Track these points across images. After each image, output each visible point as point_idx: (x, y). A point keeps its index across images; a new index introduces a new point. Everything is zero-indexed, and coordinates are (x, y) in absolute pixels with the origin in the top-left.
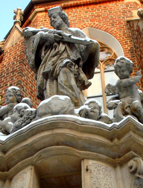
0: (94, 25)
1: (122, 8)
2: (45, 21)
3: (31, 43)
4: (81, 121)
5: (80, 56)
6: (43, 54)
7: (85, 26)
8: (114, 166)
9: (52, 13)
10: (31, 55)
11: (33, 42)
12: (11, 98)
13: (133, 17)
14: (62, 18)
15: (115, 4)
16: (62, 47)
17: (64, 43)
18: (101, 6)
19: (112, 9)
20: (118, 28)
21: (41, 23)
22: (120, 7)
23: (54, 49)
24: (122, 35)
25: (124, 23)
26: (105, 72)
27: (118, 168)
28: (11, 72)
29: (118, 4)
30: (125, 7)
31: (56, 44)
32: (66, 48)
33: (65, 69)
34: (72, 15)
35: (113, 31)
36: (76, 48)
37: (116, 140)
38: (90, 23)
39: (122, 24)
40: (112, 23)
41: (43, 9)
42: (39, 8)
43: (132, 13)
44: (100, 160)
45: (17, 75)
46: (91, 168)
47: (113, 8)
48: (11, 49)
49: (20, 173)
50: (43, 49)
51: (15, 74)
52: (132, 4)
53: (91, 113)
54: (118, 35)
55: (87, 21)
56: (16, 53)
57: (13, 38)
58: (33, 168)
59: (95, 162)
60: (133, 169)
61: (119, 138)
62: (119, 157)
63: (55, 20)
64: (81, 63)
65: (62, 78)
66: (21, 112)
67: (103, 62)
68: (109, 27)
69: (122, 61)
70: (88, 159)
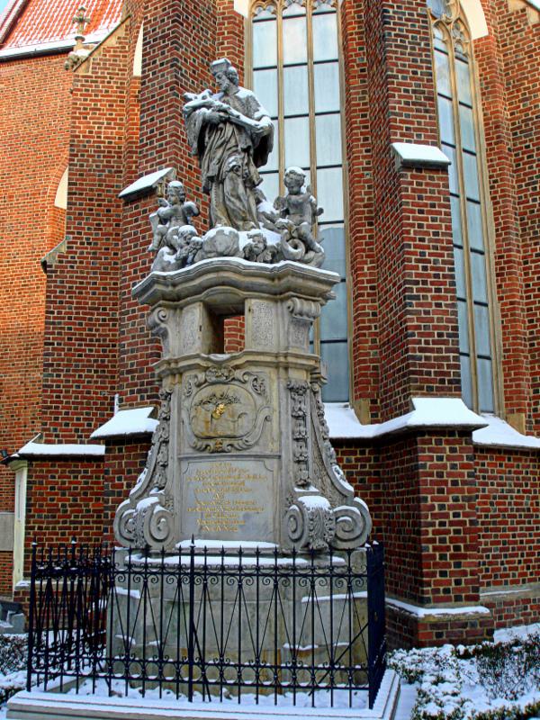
4: (244, 266)
5: (250, 144)
6: (207, 139)
8: (276, 301)
12: (173, 199)
16: (229, 129)
17: (231, 123)
23: (219, 132)
26: (314, 14)
31: (221, 125)
32: (233, 131)
33: (231, 174)
36: (245, 131)
37: (276, 281)
44: (262, 298)
46: (254, 308)
50: (207, 131)
53: (256, 249)
58: (201, 304)
62: (281, 294)
63: (220, 81)
64: (252, 152)
65: (228, 186)
69: (291, 175)
70: (251, 298)
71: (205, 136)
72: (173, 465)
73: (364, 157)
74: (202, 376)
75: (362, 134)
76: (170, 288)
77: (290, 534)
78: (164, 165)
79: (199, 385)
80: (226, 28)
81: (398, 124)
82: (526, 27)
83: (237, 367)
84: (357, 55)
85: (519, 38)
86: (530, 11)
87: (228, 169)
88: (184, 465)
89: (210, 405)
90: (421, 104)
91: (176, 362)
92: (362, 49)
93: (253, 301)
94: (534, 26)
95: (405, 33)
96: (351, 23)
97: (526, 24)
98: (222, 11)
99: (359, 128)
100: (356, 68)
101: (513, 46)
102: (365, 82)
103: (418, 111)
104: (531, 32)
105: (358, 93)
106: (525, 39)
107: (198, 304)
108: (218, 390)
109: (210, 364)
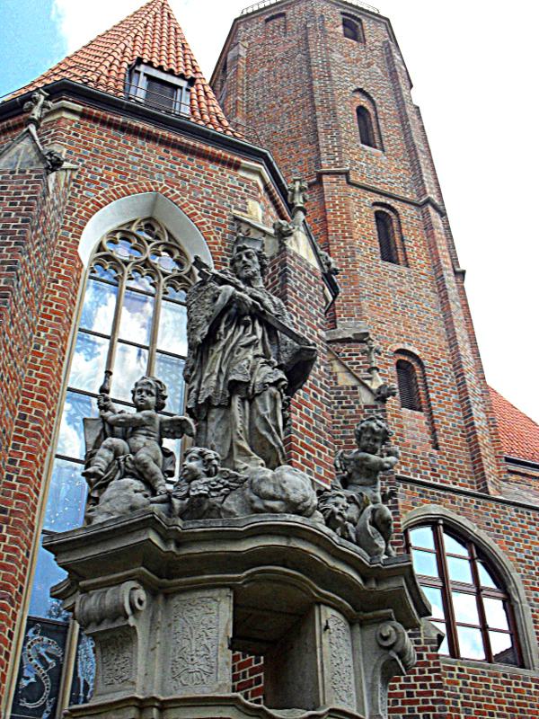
0: (172, 195)
1: (230, 183)
2: (74, 134)
3: (206, 297)
7: (152, 187)
9: (248, 246)
10: (200, 322)
11: (215, 299)
13: (246, 212)
14: (260, 263)
15: (220, 170)
18: (192, 160)
19: (212, 175)
20: (216, 224)
21: (65, 135)
22: (228, 181)
23: (242, 328)
24: (220, 241)
25: (227, 217)
27: (358, 629)
29: (225, 173)
30: (237, 185)
31: (249, 318)
33: (273, 390)
34: (134, 151)
35: (203, 223)
38: (165, 185)
39: (224, 217)
40: (206, 207)
41: (79, 108)
42: (72, 102)
43: (247, 203)
45: (12, 246)
47: (214, 175)
48: (7, 178)
50: (225, 319)
51: (8, 240)
52: (251, 185)
53: (338, 518)
54: (212, 237)
55: (159, 179)
56: (20, 193)
57: (18, 154)
59: (334, 613)
60: (390, 643)
61: (378, 581)
66: (210, 466)
67: (166, 278)
68: (199, 212)
70: (327, 605)
71: (219, 325)
76: (172, 547)
80: (64, 267)
81: (299, 447)
82: (357, 405)
85: (348, 414)
87: (271, 381)
90: (320, 433)
93: (331, 612)
94: (366, 407)
97: (357, 402)
98: (62, 246)
101: (341, 420)
103: (318, 439)
106: (355, 417)
107: (225, 591)
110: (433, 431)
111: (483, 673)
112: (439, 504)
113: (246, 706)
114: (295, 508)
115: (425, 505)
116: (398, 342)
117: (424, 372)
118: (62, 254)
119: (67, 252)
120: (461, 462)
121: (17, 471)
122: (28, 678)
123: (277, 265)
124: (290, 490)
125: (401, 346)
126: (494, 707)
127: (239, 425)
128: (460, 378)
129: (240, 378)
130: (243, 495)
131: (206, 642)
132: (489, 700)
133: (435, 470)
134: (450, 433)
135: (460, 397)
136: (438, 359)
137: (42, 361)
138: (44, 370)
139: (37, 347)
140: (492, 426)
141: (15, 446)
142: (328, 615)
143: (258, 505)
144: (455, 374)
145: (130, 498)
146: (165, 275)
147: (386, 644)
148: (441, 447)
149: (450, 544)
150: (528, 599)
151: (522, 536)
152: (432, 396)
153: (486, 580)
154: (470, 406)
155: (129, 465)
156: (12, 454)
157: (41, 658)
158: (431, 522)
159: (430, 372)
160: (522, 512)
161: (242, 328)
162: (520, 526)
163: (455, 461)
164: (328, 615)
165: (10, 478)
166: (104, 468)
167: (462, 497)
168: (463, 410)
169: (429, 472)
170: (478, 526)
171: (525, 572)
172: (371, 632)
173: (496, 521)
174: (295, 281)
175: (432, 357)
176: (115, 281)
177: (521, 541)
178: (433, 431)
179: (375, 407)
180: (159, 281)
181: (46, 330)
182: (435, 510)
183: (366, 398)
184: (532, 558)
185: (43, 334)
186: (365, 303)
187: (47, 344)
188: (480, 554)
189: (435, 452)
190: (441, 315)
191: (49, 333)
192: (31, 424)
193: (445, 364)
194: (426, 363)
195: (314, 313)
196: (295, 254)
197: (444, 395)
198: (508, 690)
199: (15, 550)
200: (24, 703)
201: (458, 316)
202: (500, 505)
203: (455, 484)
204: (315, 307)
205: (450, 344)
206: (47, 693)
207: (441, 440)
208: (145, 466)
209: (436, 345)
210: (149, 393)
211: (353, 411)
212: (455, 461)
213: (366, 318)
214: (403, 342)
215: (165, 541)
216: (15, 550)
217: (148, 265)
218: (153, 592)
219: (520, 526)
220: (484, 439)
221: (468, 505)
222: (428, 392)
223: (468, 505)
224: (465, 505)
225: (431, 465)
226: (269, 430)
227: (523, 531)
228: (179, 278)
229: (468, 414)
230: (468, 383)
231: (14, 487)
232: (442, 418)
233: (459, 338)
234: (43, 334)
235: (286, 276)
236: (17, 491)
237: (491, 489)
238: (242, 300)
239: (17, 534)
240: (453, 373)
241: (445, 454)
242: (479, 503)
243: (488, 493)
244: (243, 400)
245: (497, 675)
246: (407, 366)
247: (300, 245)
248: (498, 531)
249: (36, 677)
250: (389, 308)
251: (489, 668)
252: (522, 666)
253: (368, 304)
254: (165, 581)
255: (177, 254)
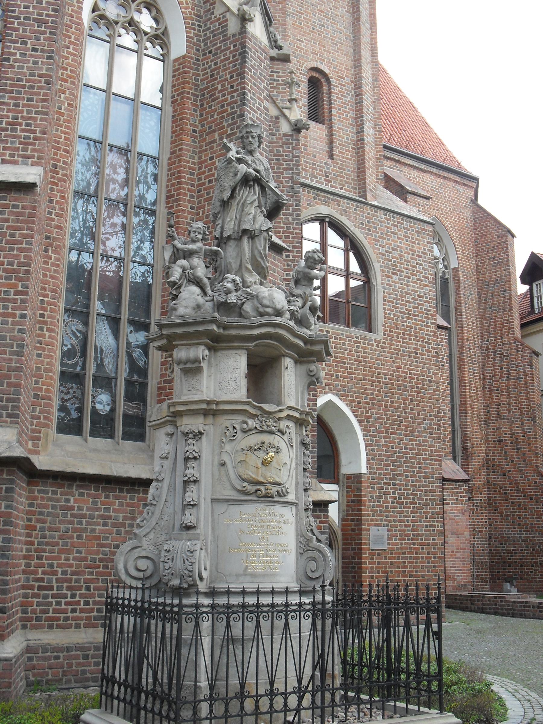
6: (237, 191)
11: (236, 175)
23: (248, 189)
24: (190, 5)
28: (35, 20)
49: (231, 351)
51: (43, 29)
53: (296, 313)
60: (313, 373)
72: (204, 506)
73: (189, 213)
74: (252, 423)
75: (189, 190)
77: (310, 575)
78: (30, 161)
79: (244, 431)
83: (280, 419)
84: (192, 115)
86: (282, 121)
88: (221, 508)
89: (261, 452)
91: (218, 403)
92: (195, 111)
94: (285, 135)
95: (255, 119)
96: (188, 83)
97: (278, 131)
99: (186, 183)
100: (189, 127)
102: (195, 142)
104: (282, 139)
105: (188, 151)
106: (275, 143)
107: (245, 351)
108: (267, 438)
109: (258, 412)
110: (331, 143)
111: (343, 335)
112: (329, 206)
113: (254, 406)
114: (279, 313)
115: (317, 206)
116: (312, 60)
117: (330, 89)
118: (71, 21)
119: (74, 19)
120: (349, 171)
121: (54, 208)
122: (66, 346)
123: (238, 43)
124: (277, 303)
125: (314, 64)
126: (346, 359)
127: (247, 255)
128: (358, 98)
129: (248, 227)
130: (253, 302)
131: (235, 374)
132: (344, 353)
133: (328, 177)
134: (344, 146)
135: (356, 115)
136: (344, 78)
137: (64, 119)
138: (67, 127)
139: (60, 108)
140: (378, 131)
141: (52, 189)
142: (288, 362)
143: (261, 310)
144: (355, 93)
145: (196, 299)
146: (146, 34)
147: (311, 374)
148: (335, 157)
149: (332, 237)
150: (382, 284)
151: (386, 235)
152: (334, 112)
153: (354, 267)
154: (363, 124)
155: (191, 276)
156: (50, 195)
157: (74, 333)
158: (321, 220)
159: (335, 90)
160: (389, 216)
161: (248, 189)
162: (386, 227)
163: (344, 170)
164: (288, 362)
165: (50, 213)
166: (178, 278)
167: (346, 201)
168: (357, 126)
169: (323, 178)
170: (355, 225)
171: (383, 263)
172: (304, 367)
173: (368, 222)
174: (251, 61)
175: (338, 76)
176: (108, 39)
177: (385, 239)
178: (331, 143)
179: (292, 136)
180: (142, 39)
181: (64, 93)
182: (324, 210)
183: (285, 128)
184: (391, 253)
185: (63, 96)
186: (289, 21)
187: (66, 105)
188: (353, 246)
189: (330, 161)
190: (352, 36)
191: (67, 95)
192: (61, 172)
193: (348, 84)
194: (333, 81)
195: (262, 87)
196: (252, 36)
197: (343, 111)
198: (358, 347)
199: (58, 266)
200: (66, 361)
201: (365, 39)
202: (373, 209)
203: (341, 189)
204: (263, 82)
205: (355, 65)
206: (78, 355)
207: (336, 152)
208: (201, 280)
209: (343, 64)
210: (199, 233)
211: (274, 137)
212: (344, 170)
213: (288, 36)
214: (316, 61)
215: (218, 327)
216: (58, 266)
217: (132, 23)
218: (210, 349)
219: (386, 227)
220: (367, 99)
221: (349, 208)
222: (331, 108)
223: (349, 208)
224: (347, 207)
225: (325, 172)
226: (262, 258)
227: (388, 231)
228: (156, 37)
229: (360, 131)
230: (365, 103)
231: (53, 220)
232: (339, 132)
233: (363, 60)
234: (63, 96)
235: (245, 57)
236: (56, 223)
237: (369, 196)
238: (250, 174)
239: (59, 254)
240: (353, 92)
241: (337, 163)
242: (358, 207)
243: (366, 199)
244: (248, 238)
245: (351, 337)
246: (317, 82)
247: (257, 28)
248: (369, 230)
249: (72, 345)
250: (308, 27)
251: (347, 332)
252: (370, 331)
253: (291, 22)
254: (216, 344)
255: (154, 12)
